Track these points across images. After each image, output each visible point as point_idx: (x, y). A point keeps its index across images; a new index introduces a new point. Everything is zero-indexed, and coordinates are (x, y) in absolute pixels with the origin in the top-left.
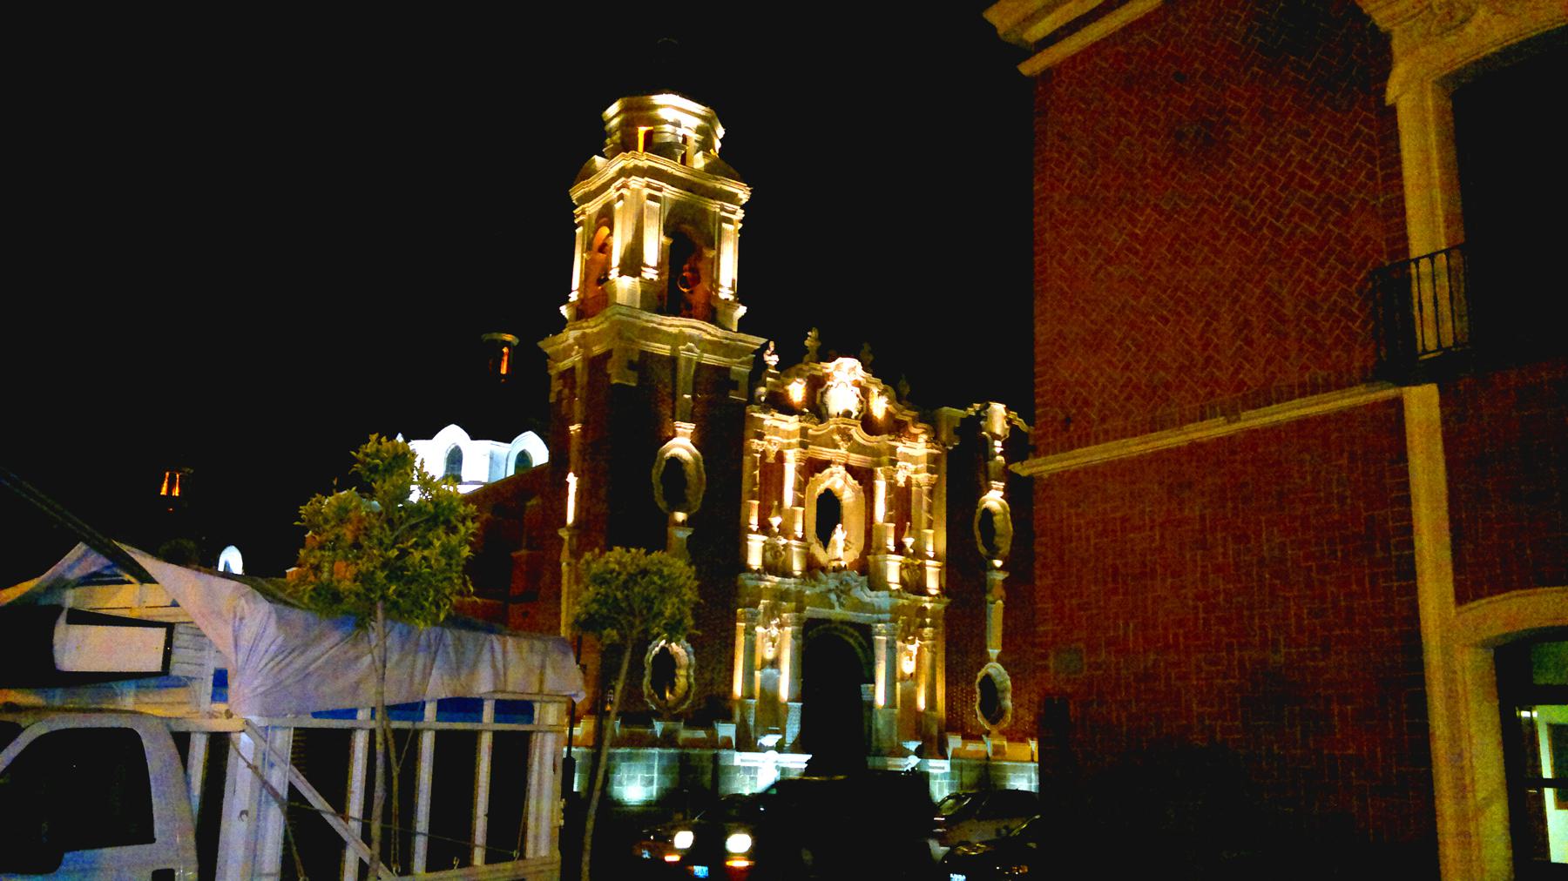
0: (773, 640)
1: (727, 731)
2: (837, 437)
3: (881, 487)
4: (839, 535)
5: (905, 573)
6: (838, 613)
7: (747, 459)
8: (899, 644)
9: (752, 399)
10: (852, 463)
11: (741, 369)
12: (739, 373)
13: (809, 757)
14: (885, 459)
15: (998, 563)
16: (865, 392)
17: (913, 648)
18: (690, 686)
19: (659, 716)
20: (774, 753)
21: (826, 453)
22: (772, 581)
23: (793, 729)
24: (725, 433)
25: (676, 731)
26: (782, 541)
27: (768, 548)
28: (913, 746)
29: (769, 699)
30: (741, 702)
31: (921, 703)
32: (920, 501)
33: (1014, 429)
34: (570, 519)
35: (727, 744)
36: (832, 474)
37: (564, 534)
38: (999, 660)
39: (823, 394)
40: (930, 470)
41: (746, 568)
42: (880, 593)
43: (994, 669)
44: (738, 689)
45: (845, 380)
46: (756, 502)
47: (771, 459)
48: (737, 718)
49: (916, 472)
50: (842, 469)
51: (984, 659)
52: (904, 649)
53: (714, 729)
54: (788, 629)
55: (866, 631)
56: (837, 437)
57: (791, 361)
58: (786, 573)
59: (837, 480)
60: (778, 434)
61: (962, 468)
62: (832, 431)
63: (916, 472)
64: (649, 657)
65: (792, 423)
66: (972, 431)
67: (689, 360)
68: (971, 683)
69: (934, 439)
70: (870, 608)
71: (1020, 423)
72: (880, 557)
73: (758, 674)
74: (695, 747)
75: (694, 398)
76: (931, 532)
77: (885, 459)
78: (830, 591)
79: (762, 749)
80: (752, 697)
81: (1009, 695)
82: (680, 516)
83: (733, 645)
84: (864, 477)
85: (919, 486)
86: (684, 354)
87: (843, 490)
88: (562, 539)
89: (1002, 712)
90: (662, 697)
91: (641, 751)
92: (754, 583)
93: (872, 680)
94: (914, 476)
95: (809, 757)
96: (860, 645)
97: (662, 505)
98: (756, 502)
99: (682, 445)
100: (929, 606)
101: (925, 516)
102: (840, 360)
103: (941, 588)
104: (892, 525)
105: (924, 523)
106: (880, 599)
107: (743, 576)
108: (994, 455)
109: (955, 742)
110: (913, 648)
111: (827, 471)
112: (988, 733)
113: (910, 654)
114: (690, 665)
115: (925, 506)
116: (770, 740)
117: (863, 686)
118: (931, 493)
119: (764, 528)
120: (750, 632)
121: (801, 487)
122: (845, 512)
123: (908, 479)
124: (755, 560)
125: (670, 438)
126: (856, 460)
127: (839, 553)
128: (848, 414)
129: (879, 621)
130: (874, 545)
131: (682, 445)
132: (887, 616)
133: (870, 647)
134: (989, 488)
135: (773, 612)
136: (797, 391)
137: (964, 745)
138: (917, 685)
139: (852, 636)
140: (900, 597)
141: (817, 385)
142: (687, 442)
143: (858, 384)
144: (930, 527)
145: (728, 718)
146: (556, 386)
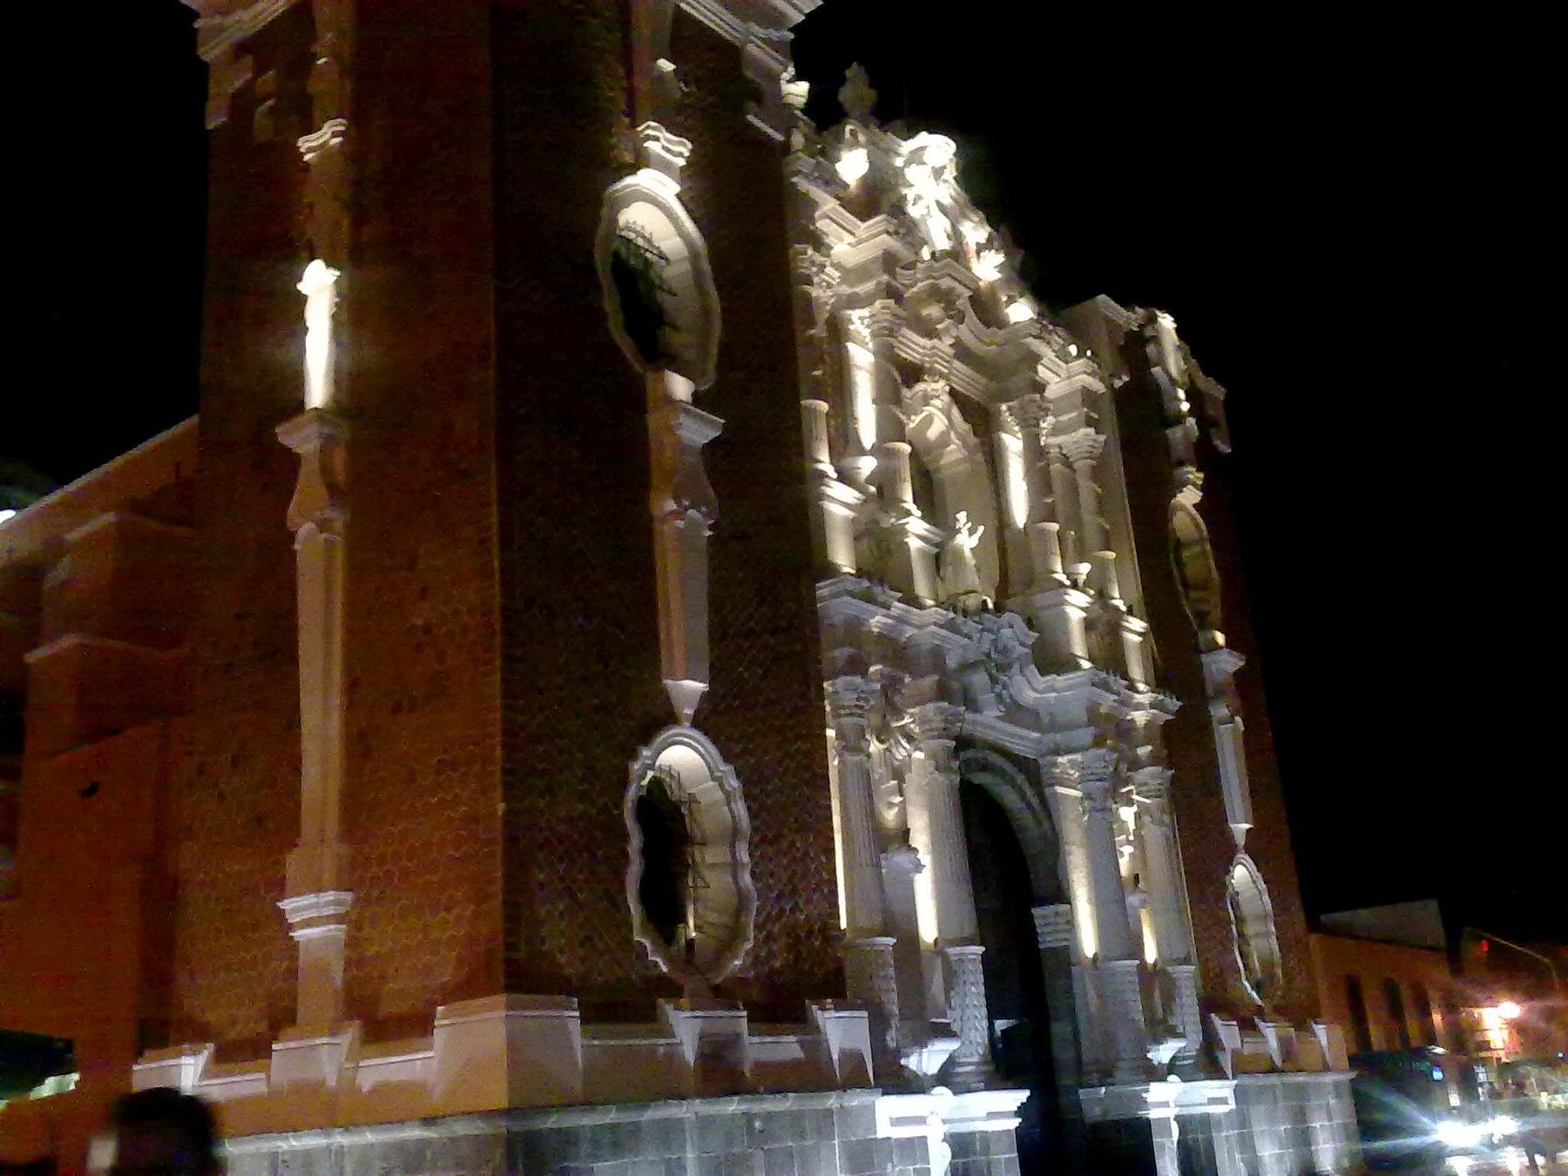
1: (841, 1030)
2: (933, 311)
13: (1023, 1095)
17: (1127, 814)
19: (671, 989)
24: (751, 210)
34: (318, 392)
36: (926, 399)
37: (301, 439)
40: (1089, 422)
41: (830, 571)
42: (1060, 680)
46: (824, 406)
50: (941, 385)
55: (1032, 772)
59: (935, 417)
64: (632, 794)
66: (1135, 351)
74: (779, 1090)
76: (1111, 555)
77: (1019, 381)
84: (979, 416)
85: (1066, 461)
88: (292, 461)
91: (650, 1115)
93: (1061, 895)
95: (1023, 1095)
100: (1140, 717)
102: (923, 138)
105: (1092, 537)
107: (824, 589)
108: (1179, 419)
114: (735, 833)
116: (928, 1059)
117: (1037, 912)
120: (853, 744)
124: (842, 556)
125: (633, 169)
127: (973, 580)
130: (1014, 576)
132: (1085, 735)
133: (1046, 809)
139: (1013, 784)
145: (835, 989)
146: (226, 84)
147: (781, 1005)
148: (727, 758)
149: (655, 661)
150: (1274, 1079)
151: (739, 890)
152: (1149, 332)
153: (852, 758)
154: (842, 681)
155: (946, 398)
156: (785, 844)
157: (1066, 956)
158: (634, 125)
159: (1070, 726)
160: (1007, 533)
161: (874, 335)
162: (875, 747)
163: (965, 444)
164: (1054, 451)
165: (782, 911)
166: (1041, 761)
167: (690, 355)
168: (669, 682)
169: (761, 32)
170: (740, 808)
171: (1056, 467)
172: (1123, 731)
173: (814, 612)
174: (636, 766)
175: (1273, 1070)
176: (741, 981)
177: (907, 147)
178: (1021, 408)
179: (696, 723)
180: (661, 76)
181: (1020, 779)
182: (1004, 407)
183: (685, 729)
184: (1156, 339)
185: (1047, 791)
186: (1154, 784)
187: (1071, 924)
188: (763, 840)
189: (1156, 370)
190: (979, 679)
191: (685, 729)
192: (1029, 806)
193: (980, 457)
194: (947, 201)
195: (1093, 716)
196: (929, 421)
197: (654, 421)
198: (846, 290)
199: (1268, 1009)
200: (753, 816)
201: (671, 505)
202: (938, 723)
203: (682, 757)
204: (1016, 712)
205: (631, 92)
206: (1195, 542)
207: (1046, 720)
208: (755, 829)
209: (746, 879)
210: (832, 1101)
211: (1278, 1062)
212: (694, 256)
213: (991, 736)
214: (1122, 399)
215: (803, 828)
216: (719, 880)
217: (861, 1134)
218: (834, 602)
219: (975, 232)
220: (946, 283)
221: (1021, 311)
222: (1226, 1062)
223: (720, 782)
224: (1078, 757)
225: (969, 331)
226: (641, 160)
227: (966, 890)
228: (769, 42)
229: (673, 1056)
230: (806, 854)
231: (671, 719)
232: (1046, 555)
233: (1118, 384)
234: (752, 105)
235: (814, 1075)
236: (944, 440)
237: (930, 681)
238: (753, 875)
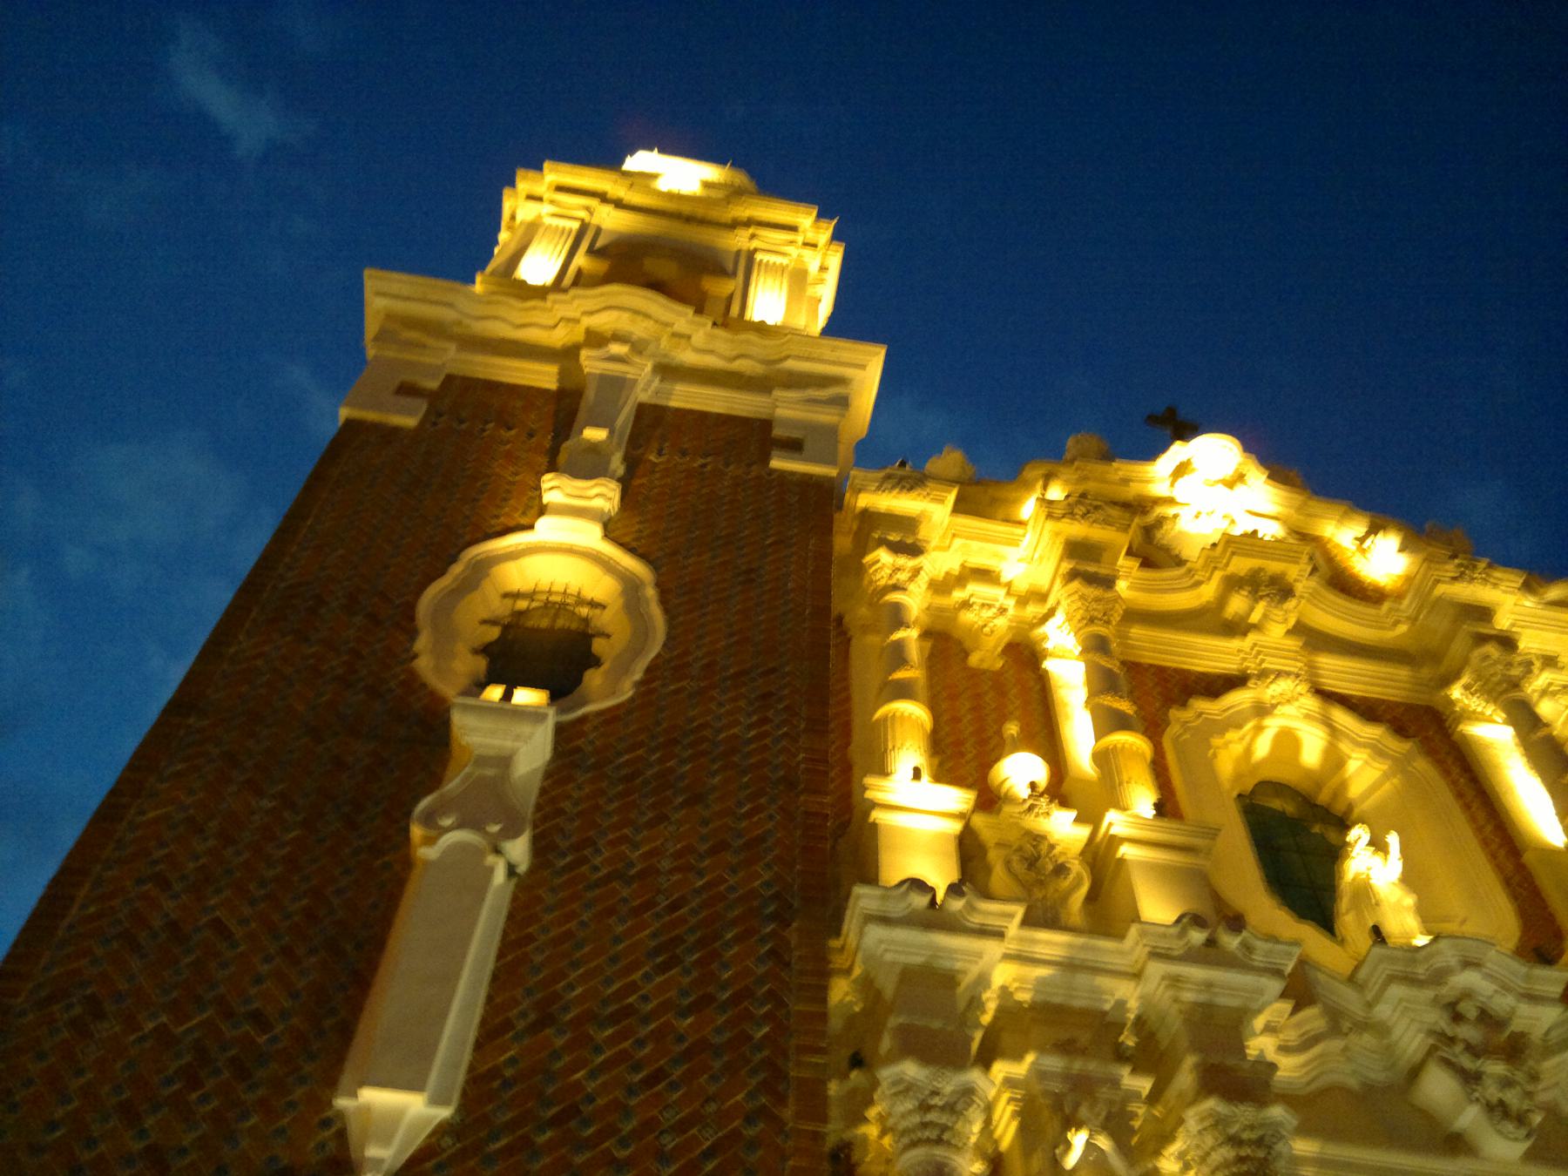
2: (1237, 604)
3: (1493, 734)
21: (1212, 654)
36: (1262, 710)
56: (1237, 604)
87: (1334, 760)
102: (1178, 451)
111: (1239, 699)
142: (590, 535)
160: (1528, 858)
163: (1378, 752)
178: (1479, 677)
182: (1456, 692)
190: (1438, 1087)
193: (1422, 765)
212: (630, 587)
236: (1334, 760)
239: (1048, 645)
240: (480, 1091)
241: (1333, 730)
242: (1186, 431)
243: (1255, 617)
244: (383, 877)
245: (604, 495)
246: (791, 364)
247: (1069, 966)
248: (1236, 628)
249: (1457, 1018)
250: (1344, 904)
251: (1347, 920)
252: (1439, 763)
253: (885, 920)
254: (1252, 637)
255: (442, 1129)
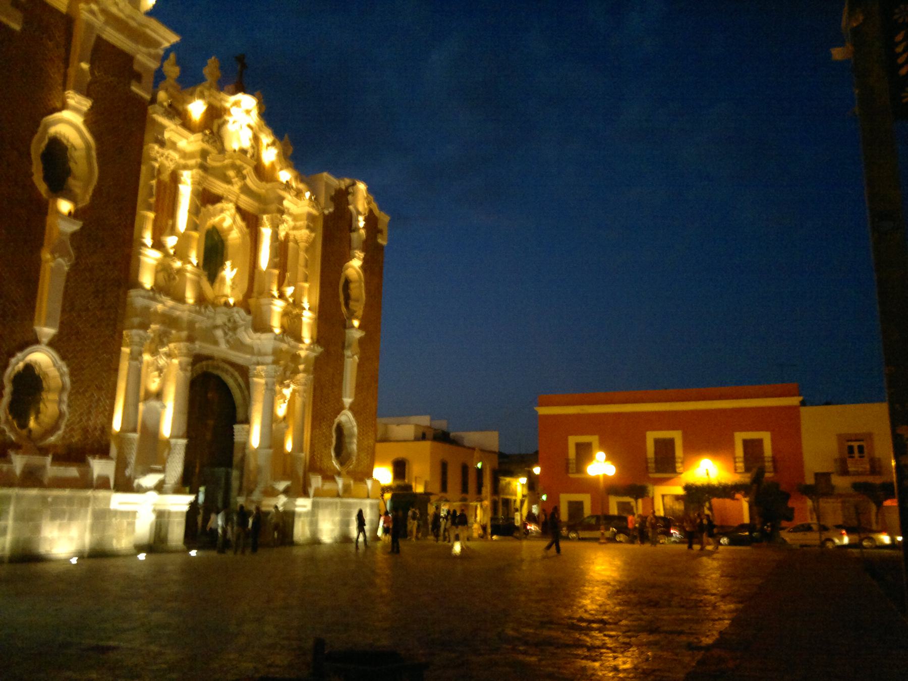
0: (160, 370)
2: (231, 173)
3: (266, 232)
4: (229, 273)
5: (285, 320)
6: (222, 349)
7: (144, 168)
8: (278, 387)
9: (154, 100)
10: (242, 205)
11: (145, 59)
12: (143, 65)
14: (273, 207)
15: (356, 323)
16: (256, 139)
17: (287, 392)
18: (61, 415)
19: (17, 447)
20: (153, 495)
21: (219, 187)
22: (163, 305)
23: (175, 468)
24: (123, 127)
25: (44, 467)
26: (178, 264)
27: (163, 269)
28: (282, 486)
29: (150, 434)
30: (120, 437)
31: (289, 446)
32: (297, 253)
33: (371, 211)
35: (103, 484)
36: (222, 211)
38: (351, 409)
39: (220, 126)
40: (308, 227)
41: (138, 285)
42: (264, 336)
43: (346, 417)
44: (117, 424)
45: (243, 114)
46: (151, 215)
47: (165, 177)
48: (114, 451)
49: (294, 228)
50: (231, 206)
51: (340, 408)
52: (281, 392)
53: (88, 465)
54: (175, 361)
55: (244, 372)
56: (231, 173)
57: (190, 82)
58: (181, 299)
59: (226, 218)
60: (176, 146)
61: (334, 227)
62: (226, 167)
63: (294, 228)
64: (10, 372)
65: (189, 143)
66: (341, 198)
67: (90, 27)
68: (330, 427)
69: (315, 201)
70: (249, 349)
71: (374, 206)
72: (264, 301)
73: (141, 407)
75: (92, 69)
76: (306, 285)
77: (273, 207)
78: (216, 327)
79: (140, 490)
80: (134, 430)
81: (355, 441)
82: (65, 206)
83: (116, 370)
84: (252, 221)
85: (296, 242)
86: (85, 15)
87: (230, 229)
89: (349, 456)
90: (24, 425)
92: (146, 302)
93: (247, 421)
94: (292, 233)
96: (239, 386)
97: (42, 188)
98: (151, 215)
99: (70, 122)
100: (303, 353)
101: (301, 270)
102: (240, 96)
103: (312, 338)
104: (276, 272)
105: (300, 276)
106: (264, 341)
107: (133, 293)
108: (357, 229)
109: (316, 481)
110: (287, 392)
111: (219, 206)
112: (339, 474)
113: (284, 397)
114: (63, 389)
115: (301, 261)
116: (151, 480)
118: (307, 250)
119: (158, 245)
120: (136, 357)
121: (195, 211)
122: (230, 251)
123: (287, 235)
124: (147, 280)
125: (60, 110)
126: (246, 202)
128: (244, 152)
129: (258, 364)
130: (256, 288)
131: (70, 122)
132: (270, 359)
134: (351, 257)
135: (162, 339)
136: (197, 109)
137: (323, 485)
138: (287, 427)
139: (232, 376)
140: (282, 340)
141: (215, 114)
142: (78, 120)
143: (250, 127)
144: (306, 281)
145: (103, 452)
147: (73, 456)
148: (63, 358)
149: (32, 319)
150: (337, 500)
151: (60, 411)
152: (350, 190)
153: (134, 363)
154: (134, 332)
155: (233, 211)
156: (88, 395)
157: (245, 445)
158: (64, 89)
159: (265, 355)
160: (256, 271)
161: (193, 184)
162: (147, 357)
163: (241, 231)
164: (291, 237)
165: (81, 420)
166: (251, 367)
167: (78, 191)
168: (37, 328)
169: (144, 49)
170: (67, 380)
171: (291, 244)
172: (295, 358)
173: (125, 302)
174: (13, 360)
175: (338, 496)
176: (54, 446)
177: (232, 99)
179: (52, 344)
180: (82, 70)
181: (236, 374)
182: (265, 217)
183: (43, 347)
184: (354, 194)
185: (250, 379)
186: (303, 381)
187: (248, 433)
188: (78, 392)
189: (351, 207)
190: (219, 333)
191: (43, 347)
192: (239, 386)
193: (248, 238)
194: (253, 124)
195: (277, 354)
196: (223, 220)
197: (50, 219)
198: (182, 162)
199: (344, 473)
200: (73, 382)
201: (48, 256)
202: (184, 351)
203: (41, 357)
204: (240, 346)
205: (65, 76)
206: (356, 282)
207: (256, 350)
208: (73, 388)
209: (64, 407)
210: (90, 493)
211: (341, 493)
212: (88, 147)
213: (223, 355)
214: (327, 219)
215: (99, 388)
216: (51, 405)
217: (102, 506)
218: (136, 299)
219: (266, 138)
220: (238, 162)
221: (285, 175)
222: (311, 492)
223: (59, 370)
224: (264, 367)
225: (252, 182)
226: (64, 106)
227: (184, 419)
228: (149, 55)
229: (11, 472)
230: (99, 399)
231: (35, 341)
232: (271, 282)
233: (326, 212)
234: (134, 82)
235: (86, 483)
236: (230, 229)
237: (184, 334)
238: (69, 406)
239: (183, 179)
240: (63, 326)
241: (234, 221)
242: (245, 91)
243: (233, 180)
244: (36, 265)
245: (86, 104)
246: (148, 31)
247: (172, 308)
248: (228, 181)
249: (229, 320)
250: (218, 280)
251: (217, 285)
252: (251, 239)
253: (144, 297)
254: (230, 186)
255: (55, 336)
